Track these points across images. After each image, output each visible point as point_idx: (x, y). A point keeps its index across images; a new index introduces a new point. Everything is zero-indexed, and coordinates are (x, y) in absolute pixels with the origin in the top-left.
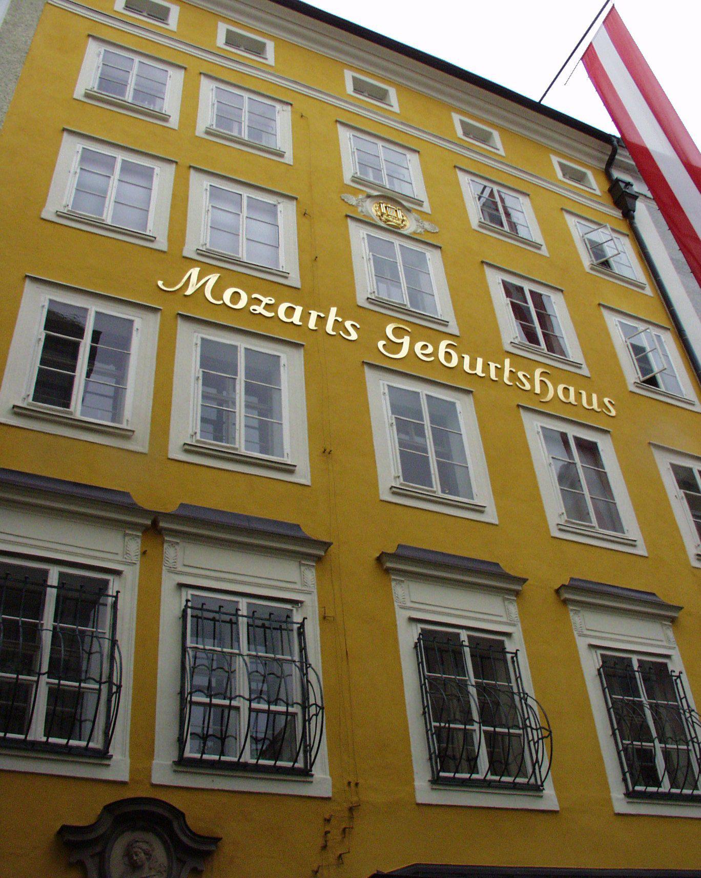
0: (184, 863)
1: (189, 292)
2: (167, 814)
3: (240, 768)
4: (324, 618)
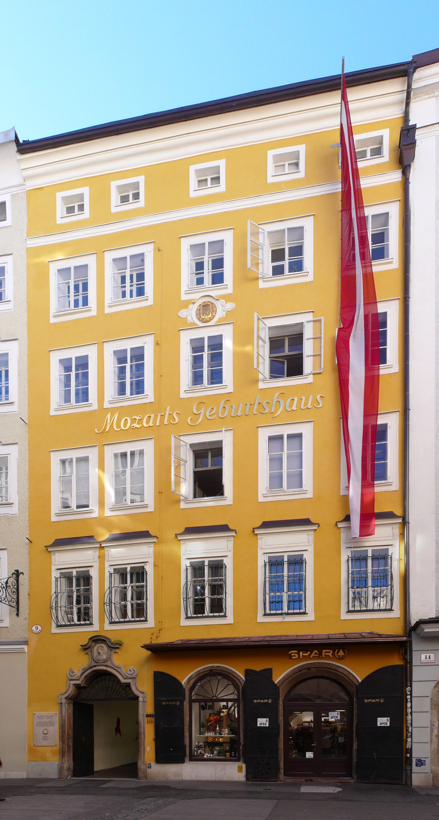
0: (112, 650)
1: (107, 430)
2: (104, 639)
3: (129, 622)
4: (155, 566)
